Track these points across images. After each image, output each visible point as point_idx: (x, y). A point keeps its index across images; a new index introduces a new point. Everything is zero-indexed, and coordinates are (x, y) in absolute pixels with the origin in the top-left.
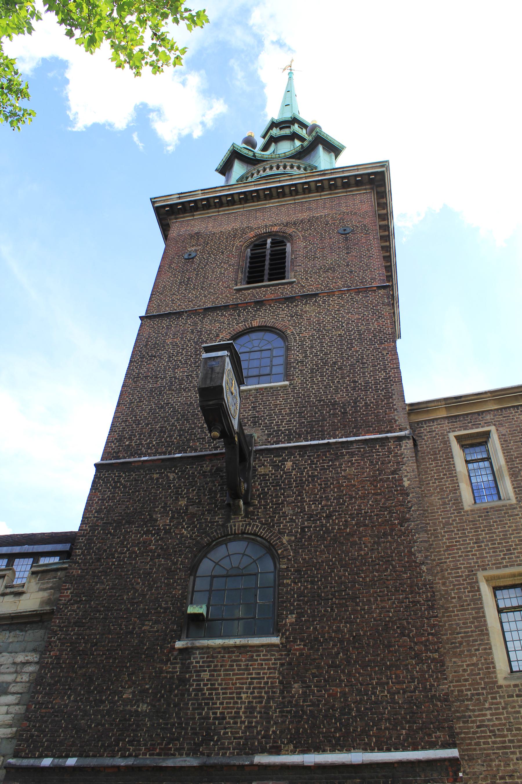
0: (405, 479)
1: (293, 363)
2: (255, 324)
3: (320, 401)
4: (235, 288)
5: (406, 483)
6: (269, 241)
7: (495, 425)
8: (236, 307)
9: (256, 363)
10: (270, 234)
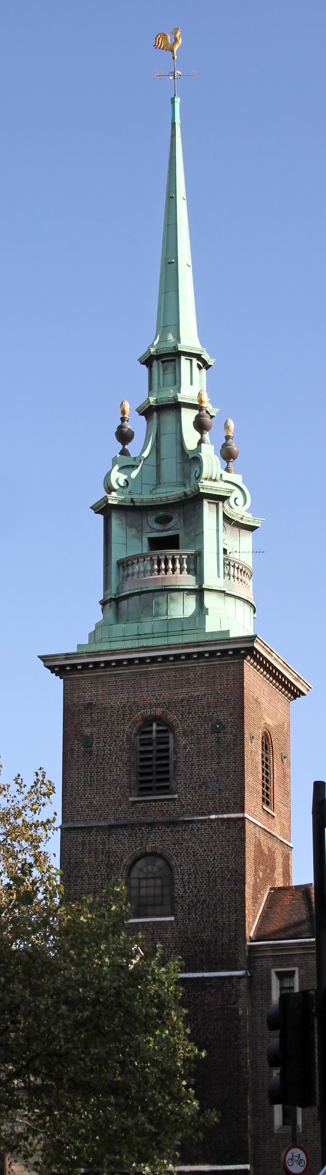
0: (240, 1009)
1: (177, 897)
2: (149, 850)
3: (194, 937)
4: (131, 799)
5: (240, 1012)
6: (154, 727)
7: (298, 966)
8: (133, 825)
9: (151, 891)
10: (156, 719)
